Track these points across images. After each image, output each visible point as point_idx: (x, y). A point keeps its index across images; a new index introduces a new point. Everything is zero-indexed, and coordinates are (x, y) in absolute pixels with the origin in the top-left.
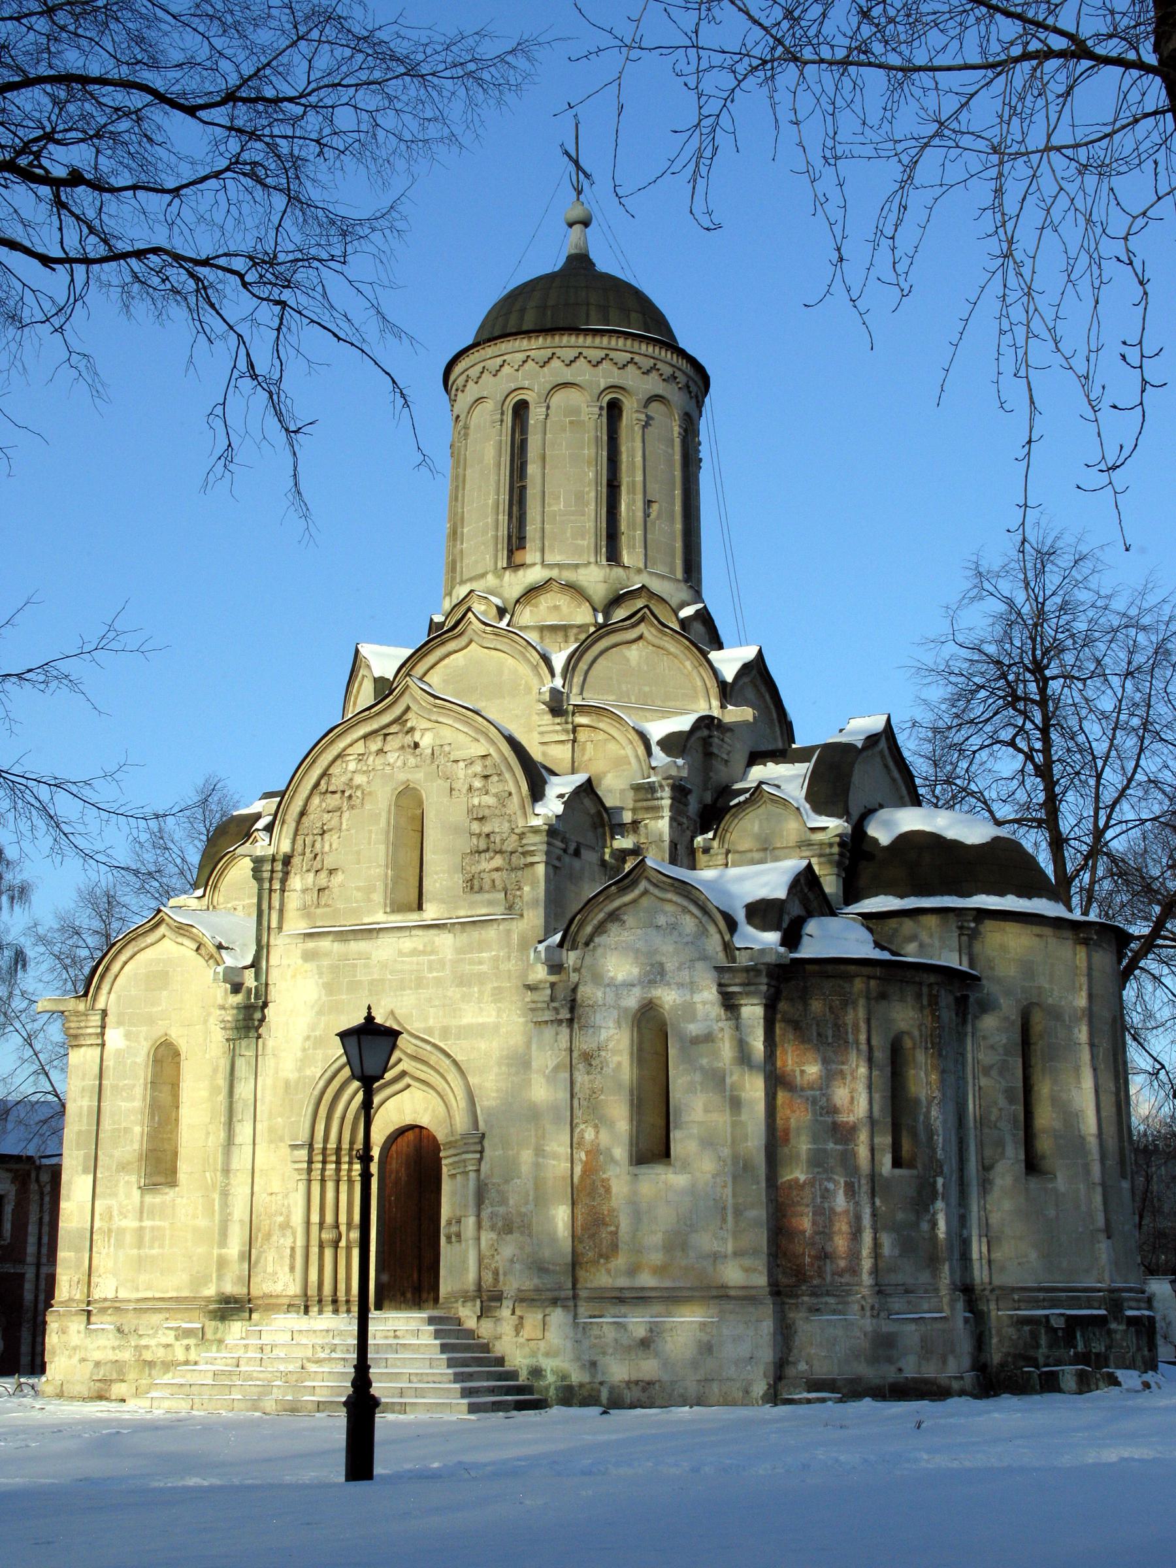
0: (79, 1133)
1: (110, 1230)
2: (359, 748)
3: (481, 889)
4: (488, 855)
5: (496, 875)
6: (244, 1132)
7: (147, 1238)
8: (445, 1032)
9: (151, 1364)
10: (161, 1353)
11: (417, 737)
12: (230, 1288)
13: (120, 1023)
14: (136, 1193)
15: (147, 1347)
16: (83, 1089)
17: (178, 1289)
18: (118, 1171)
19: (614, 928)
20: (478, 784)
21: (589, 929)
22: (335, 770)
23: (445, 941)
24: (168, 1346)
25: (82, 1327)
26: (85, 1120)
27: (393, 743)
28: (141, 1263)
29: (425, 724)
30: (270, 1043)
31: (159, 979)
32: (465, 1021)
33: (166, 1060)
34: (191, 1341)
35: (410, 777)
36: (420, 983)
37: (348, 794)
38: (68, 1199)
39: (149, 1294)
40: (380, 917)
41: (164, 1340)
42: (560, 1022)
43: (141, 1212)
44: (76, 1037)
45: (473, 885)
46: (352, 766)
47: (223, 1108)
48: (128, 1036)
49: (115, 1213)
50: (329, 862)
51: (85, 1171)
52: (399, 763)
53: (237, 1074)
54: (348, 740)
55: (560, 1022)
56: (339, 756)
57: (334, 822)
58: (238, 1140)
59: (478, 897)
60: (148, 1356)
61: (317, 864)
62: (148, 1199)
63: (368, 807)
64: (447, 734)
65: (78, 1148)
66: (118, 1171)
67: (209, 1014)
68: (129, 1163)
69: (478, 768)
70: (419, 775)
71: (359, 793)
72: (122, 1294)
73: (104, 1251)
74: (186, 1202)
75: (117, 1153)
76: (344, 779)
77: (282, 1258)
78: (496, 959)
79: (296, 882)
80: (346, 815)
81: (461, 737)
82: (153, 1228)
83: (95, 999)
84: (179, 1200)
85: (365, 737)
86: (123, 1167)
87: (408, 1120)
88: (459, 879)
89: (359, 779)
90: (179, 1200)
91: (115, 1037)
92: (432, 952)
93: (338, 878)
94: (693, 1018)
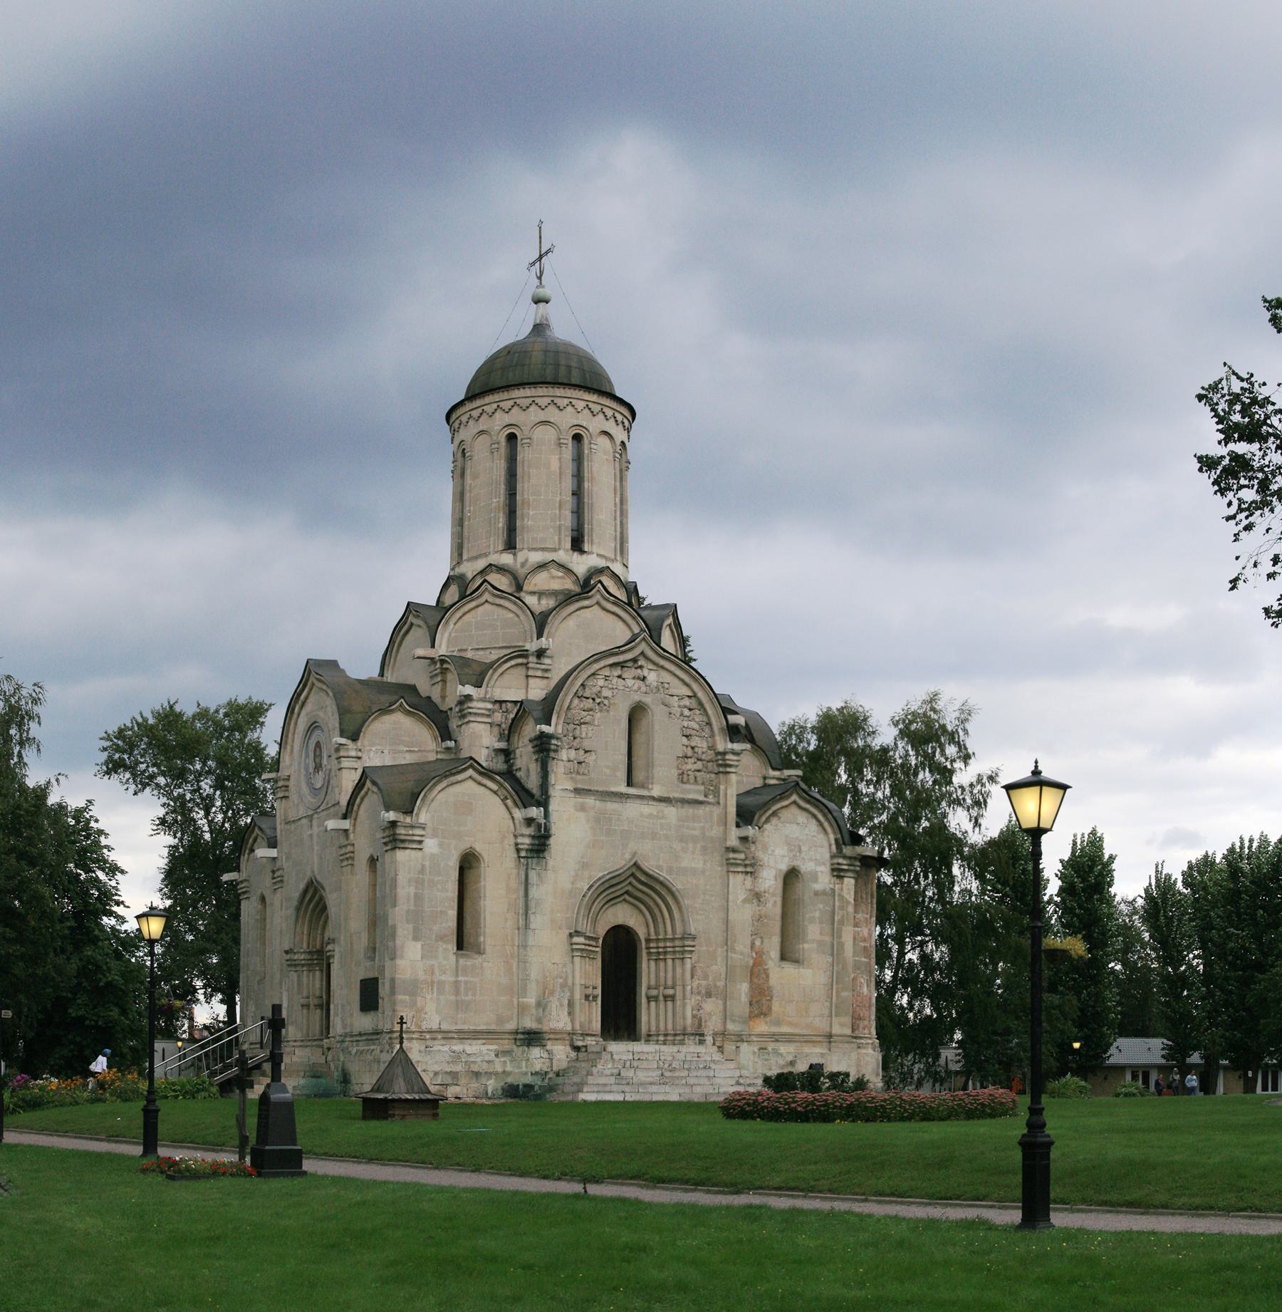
0: (408, 911)
1: (433, 982)
2: (607, 672)
3: (688, 782)
4: (692, 760)
5: (698, 774)
6: (536, 921)
7: (462, 989)
8: (670, 870)
9: (477, 1074)
10: (485, 1067)
11: (645, 672)
12: (529, 1024)
13: (434, 836)
14: (453, 958)
15: (474, 1062)
16: (410, 881)
17: (486, 1024)
18: (437, 941)
19: (774, 821)
20: (686, 712)
21: (764, 819)
22: (590, 683)
23: (671, 812)
24: (488, 1062)
25: (423, 1048)
26: (412, 902)
27: (629, 673)
28: (459, 1006)
29: (651, 666)
30: (551, 863)
31: (465, 808)
32: (684, 864)
33: (468, 864)
34: (506, 1059)
35: (644, 700)
36: (654, 836)
37: (599, 702)
38: (402, 957)
39: (466, 1027)
40: (623, 788)
41: (487, 1058)
42: (747, 873)
43: (457, 971)
44: (403, 841)
45: (682, 777)
46: (601, 682)
47: (521, 902)
48: (441, 845)
49: (437, 971)
50: (587, 744)
51: (416, 938)
52: (635, 688)
53: (530, 881)
54: (602, 663)
55: (747, 873)
56: (593, 674)
57: (588, 719)
58: (532, 926)
59: (687, 786)
60: (476, 1069)
61: (575, 743)
62: (462, 961)
63: (612, 713)
64: (667, 677)
65: (408, 922)
66: (437, 941)
67: (504, 837)
68: (445, 935)
69: (687, 702)
70: (647, 700)
71: (606, 702)
72: (444, 1027)
73: (428, 997)
74: (490, 966)
75: (435, 928)
76: (595, 690)
77: (562, 1005)
78: (703, 828)
79: (564, 755)
80: (598, 715)
81: (676, 681)
82: (466, 982)
83: (417, 815)
84: (485, 964)
85: (611, 665)
86: (441, 938)
87: (620, 922)
88: (675, 772)
89: (606, 693)
90: (485, 964)
91: (431, 845)
92: (662, 818)
93: (591, 758)
94: (816, 880)
